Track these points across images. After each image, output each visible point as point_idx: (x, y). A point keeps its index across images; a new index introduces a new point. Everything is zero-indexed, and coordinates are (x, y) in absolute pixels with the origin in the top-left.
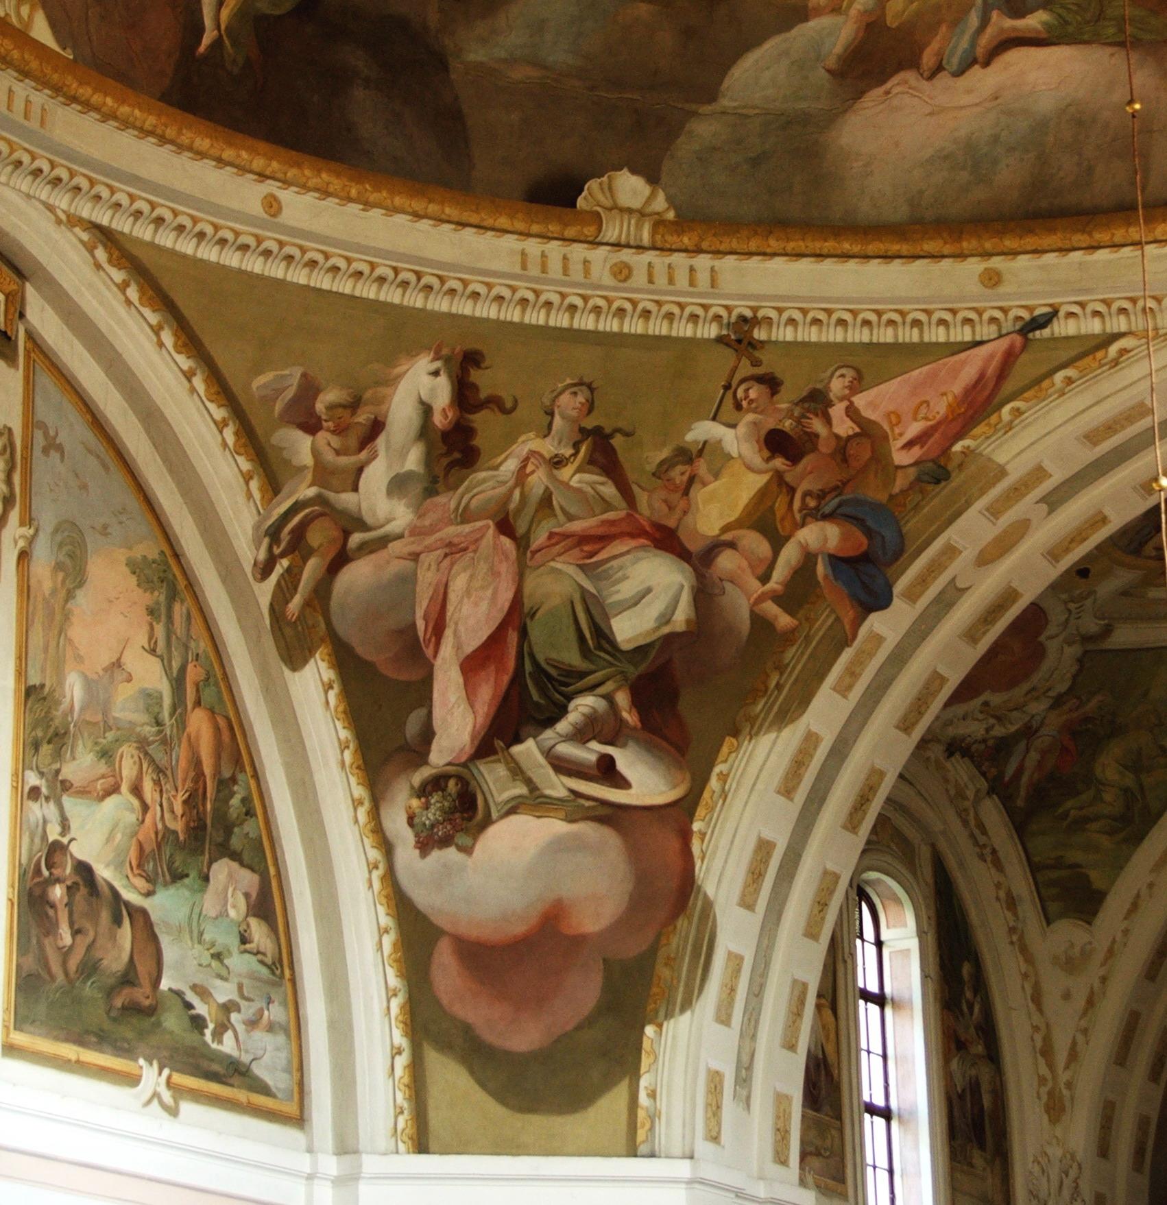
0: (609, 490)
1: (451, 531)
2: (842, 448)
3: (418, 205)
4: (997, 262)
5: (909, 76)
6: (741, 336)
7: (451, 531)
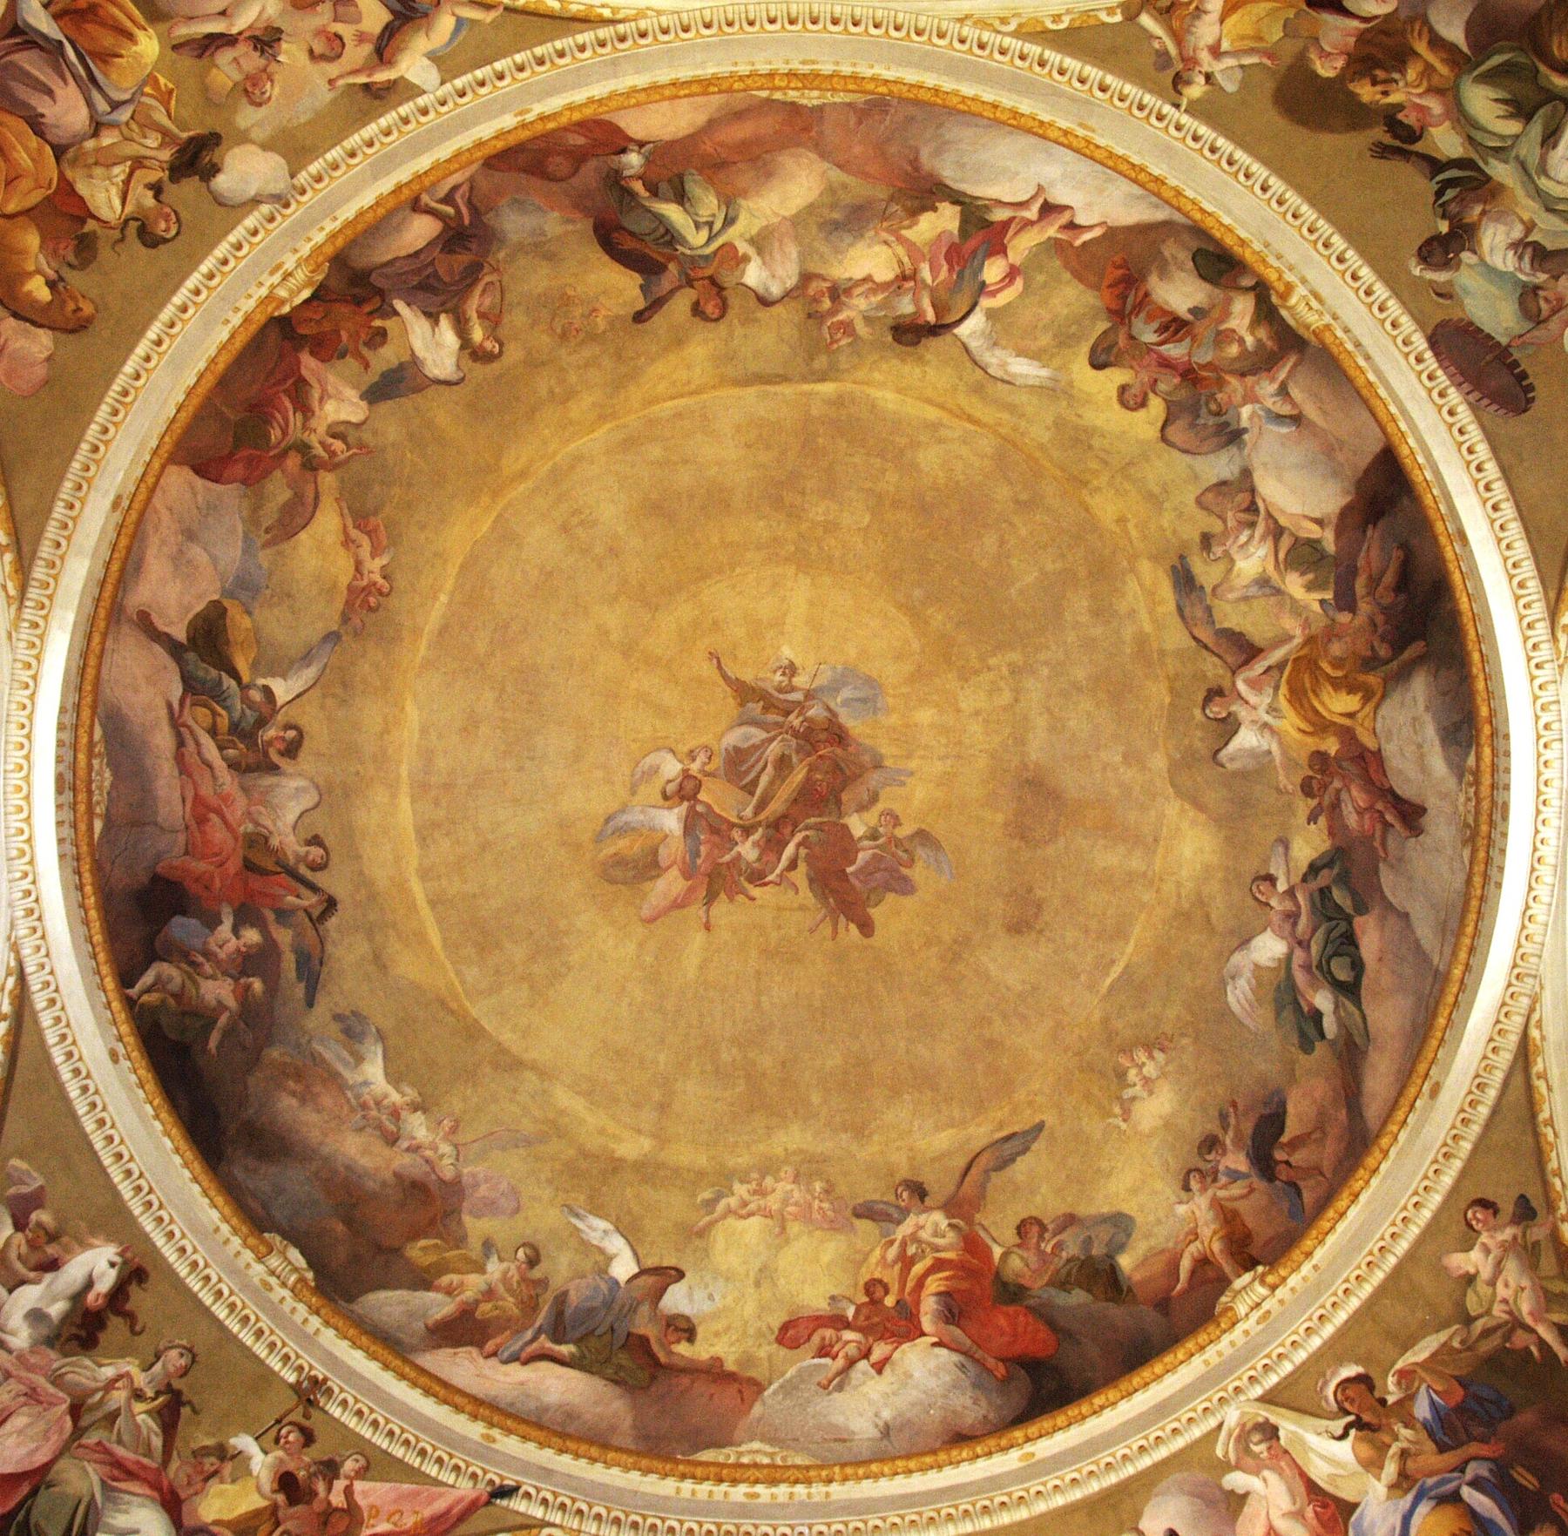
0: (157, 1442)
1: (41, 1381)
2: (330, 1512)
3: (183, 1145)
4: (495, 1432)
5: (474, 1351)
6: (310, 1392)
7: (41, 1381)
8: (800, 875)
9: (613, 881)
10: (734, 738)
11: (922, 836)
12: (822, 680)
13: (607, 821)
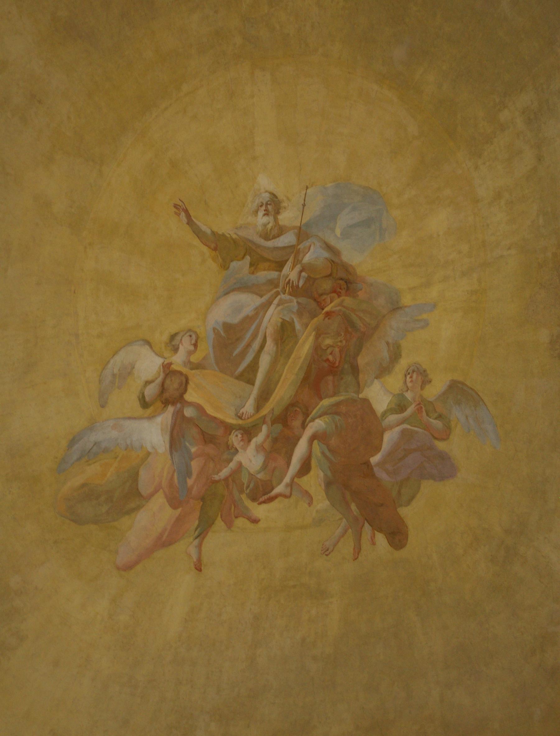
8: (314, 482)
9: (78, 520)
10: (225, 311)
11: (458, 390)
12: (315, 209)
13: (72, 442)
